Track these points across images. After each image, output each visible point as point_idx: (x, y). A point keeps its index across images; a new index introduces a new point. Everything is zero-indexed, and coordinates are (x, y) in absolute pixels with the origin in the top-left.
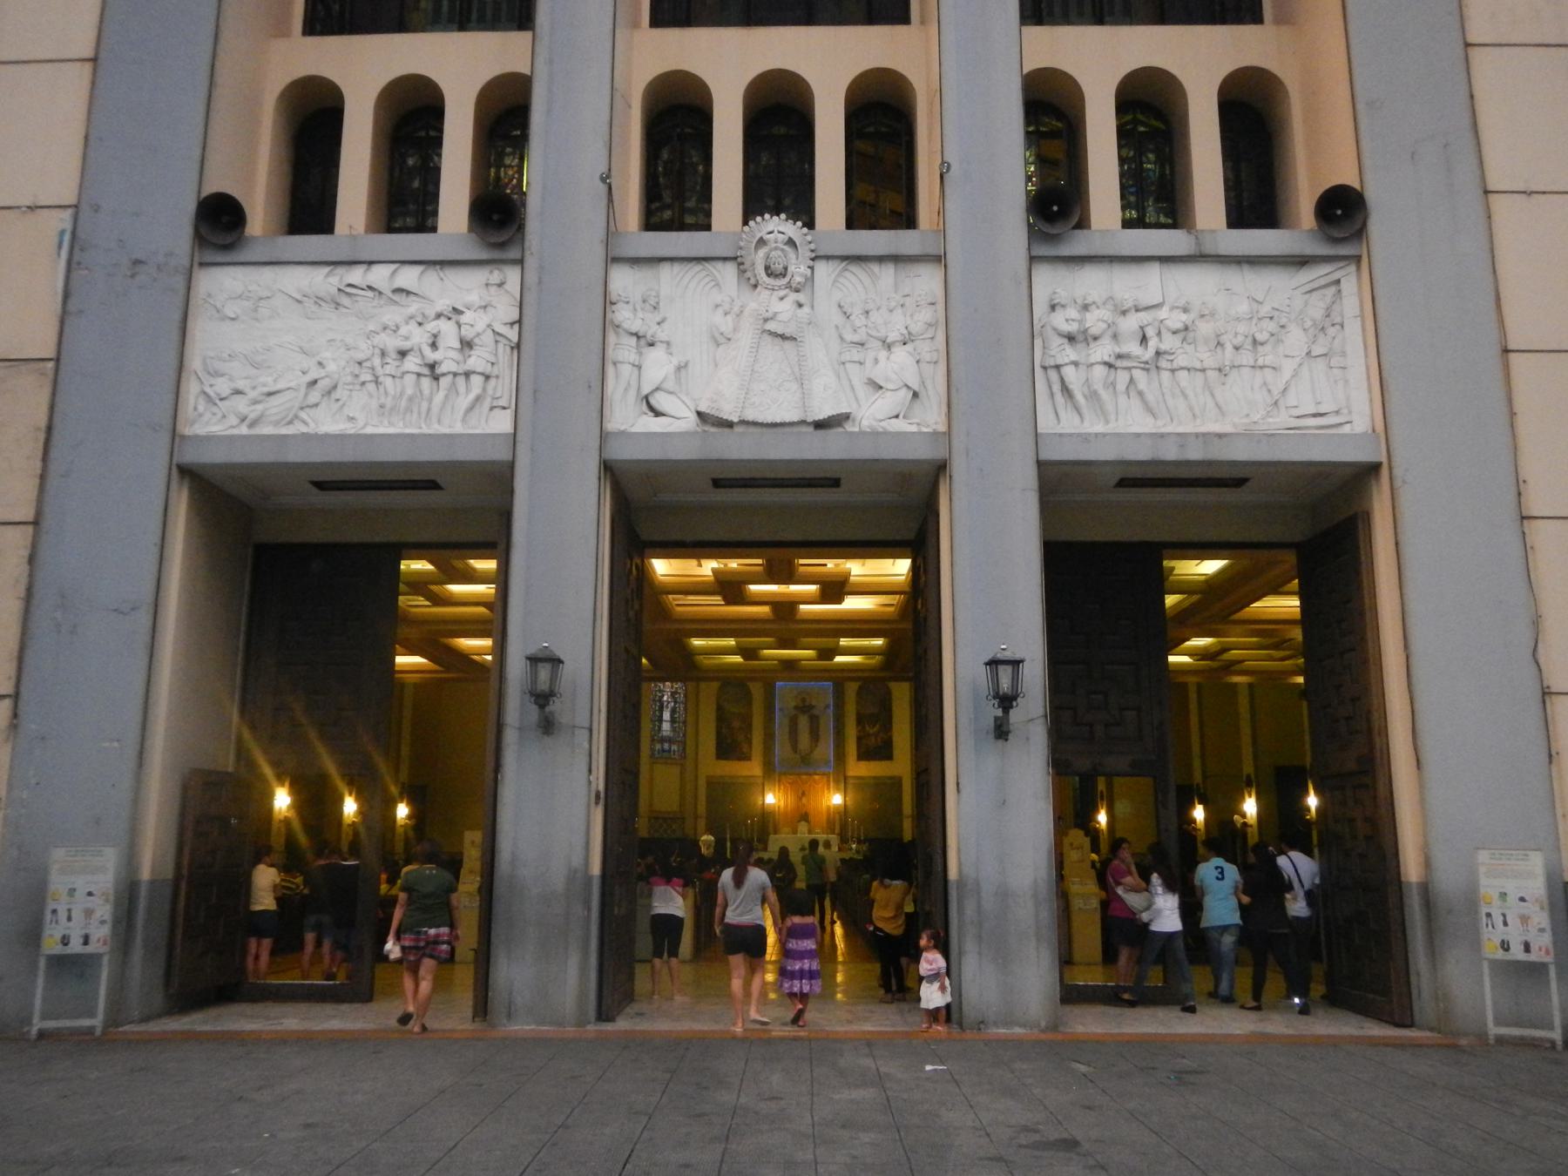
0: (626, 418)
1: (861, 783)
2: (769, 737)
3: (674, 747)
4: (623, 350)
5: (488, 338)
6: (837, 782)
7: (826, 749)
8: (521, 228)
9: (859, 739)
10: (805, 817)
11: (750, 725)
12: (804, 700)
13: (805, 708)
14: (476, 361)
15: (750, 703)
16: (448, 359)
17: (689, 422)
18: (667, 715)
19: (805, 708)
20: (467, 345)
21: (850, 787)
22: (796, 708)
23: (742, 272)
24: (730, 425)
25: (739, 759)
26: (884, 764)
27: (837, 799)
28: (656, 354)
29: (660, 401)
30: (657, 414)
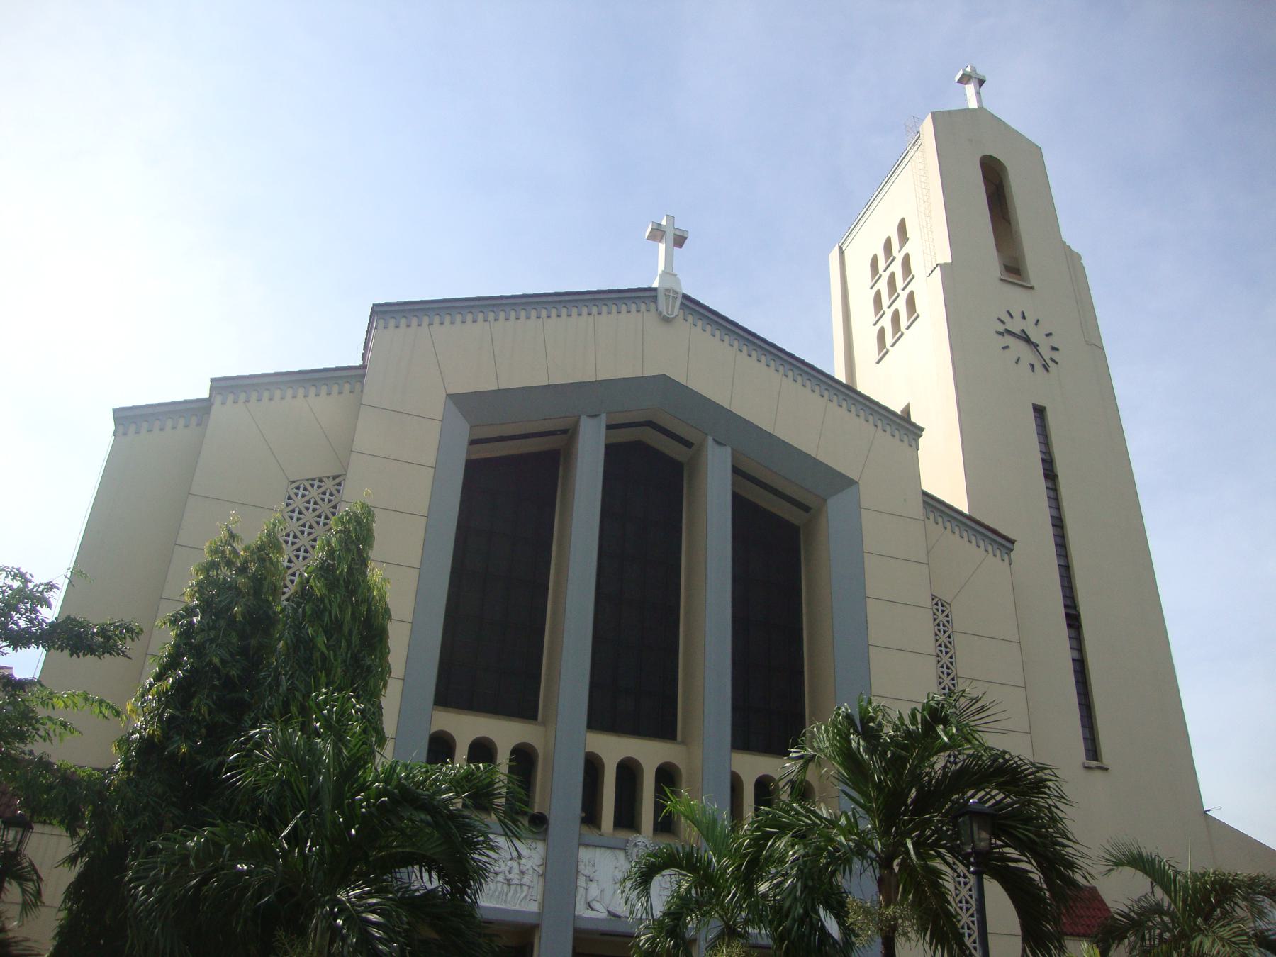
0: (581, 911)
4: (581, 882)
5: (531, 871)
8: (547, 829)
14: (526, 880)
16: (514, 876)
17: (604, 915)
20: (522, 873)
23: (626, 856)
24: (619, 917)
28: (593, 885)
29: (596, 905)
30: (593, 909)
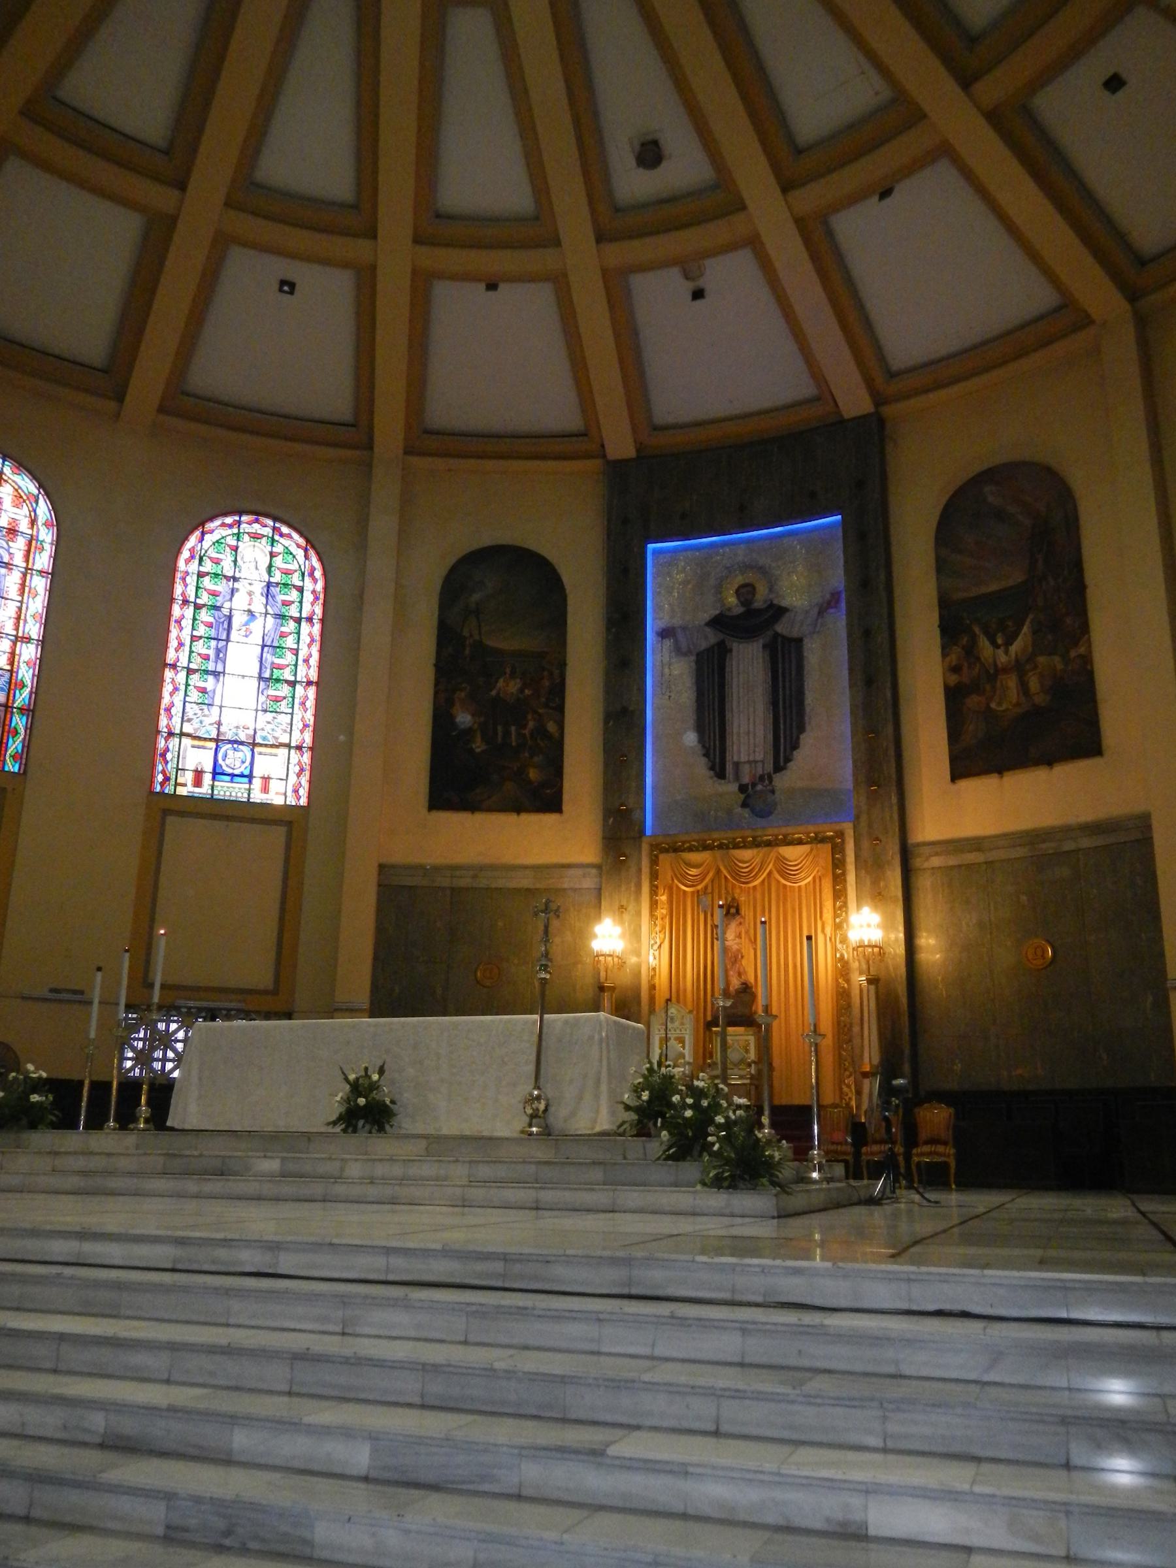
1: (974, 863)
2: (623, 722)
3: (270, 764)
6: (871, 867)
7: (829, 748)
9: (954, 696)
10: (739, 1009)
11: (559, 690)
12: (746, 592)
13: (752, 620)
15: (557, 622)
18: (243, 656)
19: (752, 620)
21: (925, 884)
22: (719, 622)
25: (518, 809)
26: (1065, 772)
27: (868, 926)
